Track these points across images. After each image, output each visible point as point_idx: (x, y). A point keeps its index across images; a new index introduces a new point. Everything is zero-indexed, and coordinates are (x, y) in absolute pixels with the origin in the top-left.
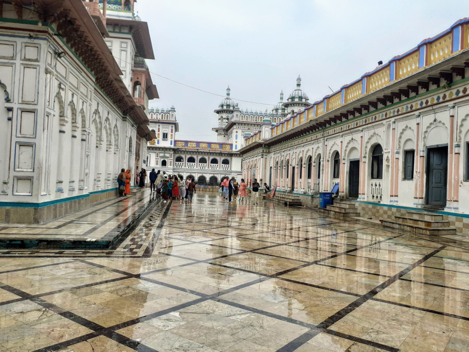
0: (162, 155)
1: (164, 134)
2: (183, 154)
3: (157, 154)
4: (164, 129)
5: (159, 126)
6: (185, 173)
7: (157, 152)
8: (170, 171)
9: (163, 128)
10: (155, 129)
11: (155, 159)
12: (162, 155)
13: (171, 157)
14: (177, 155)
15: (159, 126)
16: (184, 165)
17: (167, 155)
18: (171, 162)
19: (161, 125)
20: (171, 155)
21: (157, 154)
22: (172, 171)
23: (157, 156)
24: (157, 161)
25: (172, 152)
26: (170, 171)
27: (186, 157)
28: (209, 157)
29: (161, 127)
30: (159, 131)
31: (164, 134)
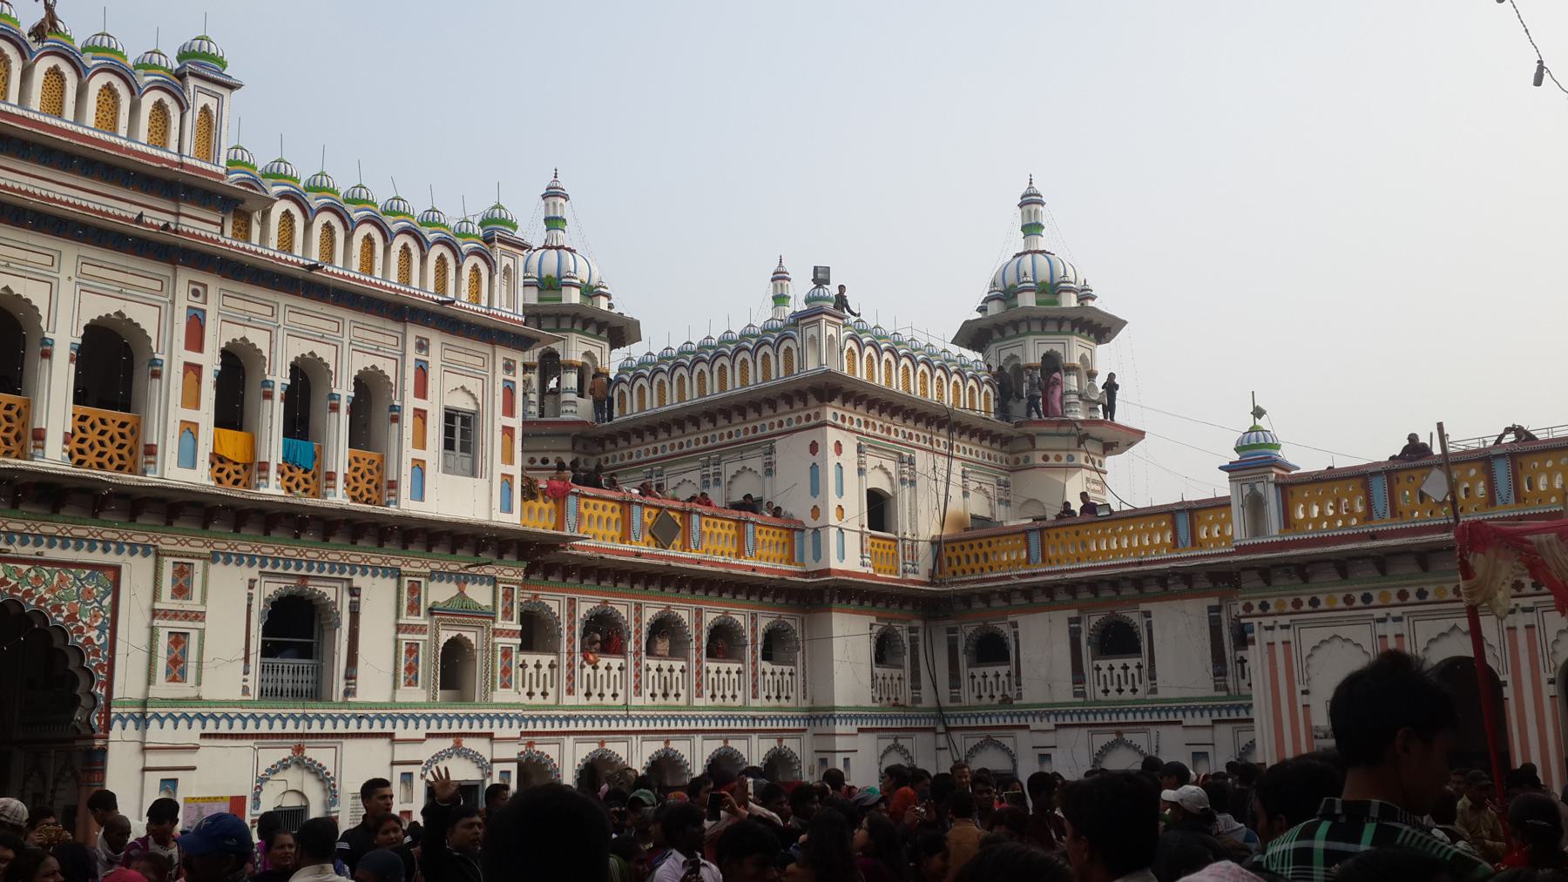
0: (440, 593)
1: (450, 415)
4: (454, 381)
5: (422, 346)
7: (414, 565)
9: (449, 366)
10: (388, 368)
12: (440, 593)
15: (422, 346)
17: (480, 595)
19: (436, 339)
20: (508, 594)
21: (415, 589)
23: (414, 608)
25: (511, 572)
28: (699, 613)
29: (434, 359)
30: (421, 391)
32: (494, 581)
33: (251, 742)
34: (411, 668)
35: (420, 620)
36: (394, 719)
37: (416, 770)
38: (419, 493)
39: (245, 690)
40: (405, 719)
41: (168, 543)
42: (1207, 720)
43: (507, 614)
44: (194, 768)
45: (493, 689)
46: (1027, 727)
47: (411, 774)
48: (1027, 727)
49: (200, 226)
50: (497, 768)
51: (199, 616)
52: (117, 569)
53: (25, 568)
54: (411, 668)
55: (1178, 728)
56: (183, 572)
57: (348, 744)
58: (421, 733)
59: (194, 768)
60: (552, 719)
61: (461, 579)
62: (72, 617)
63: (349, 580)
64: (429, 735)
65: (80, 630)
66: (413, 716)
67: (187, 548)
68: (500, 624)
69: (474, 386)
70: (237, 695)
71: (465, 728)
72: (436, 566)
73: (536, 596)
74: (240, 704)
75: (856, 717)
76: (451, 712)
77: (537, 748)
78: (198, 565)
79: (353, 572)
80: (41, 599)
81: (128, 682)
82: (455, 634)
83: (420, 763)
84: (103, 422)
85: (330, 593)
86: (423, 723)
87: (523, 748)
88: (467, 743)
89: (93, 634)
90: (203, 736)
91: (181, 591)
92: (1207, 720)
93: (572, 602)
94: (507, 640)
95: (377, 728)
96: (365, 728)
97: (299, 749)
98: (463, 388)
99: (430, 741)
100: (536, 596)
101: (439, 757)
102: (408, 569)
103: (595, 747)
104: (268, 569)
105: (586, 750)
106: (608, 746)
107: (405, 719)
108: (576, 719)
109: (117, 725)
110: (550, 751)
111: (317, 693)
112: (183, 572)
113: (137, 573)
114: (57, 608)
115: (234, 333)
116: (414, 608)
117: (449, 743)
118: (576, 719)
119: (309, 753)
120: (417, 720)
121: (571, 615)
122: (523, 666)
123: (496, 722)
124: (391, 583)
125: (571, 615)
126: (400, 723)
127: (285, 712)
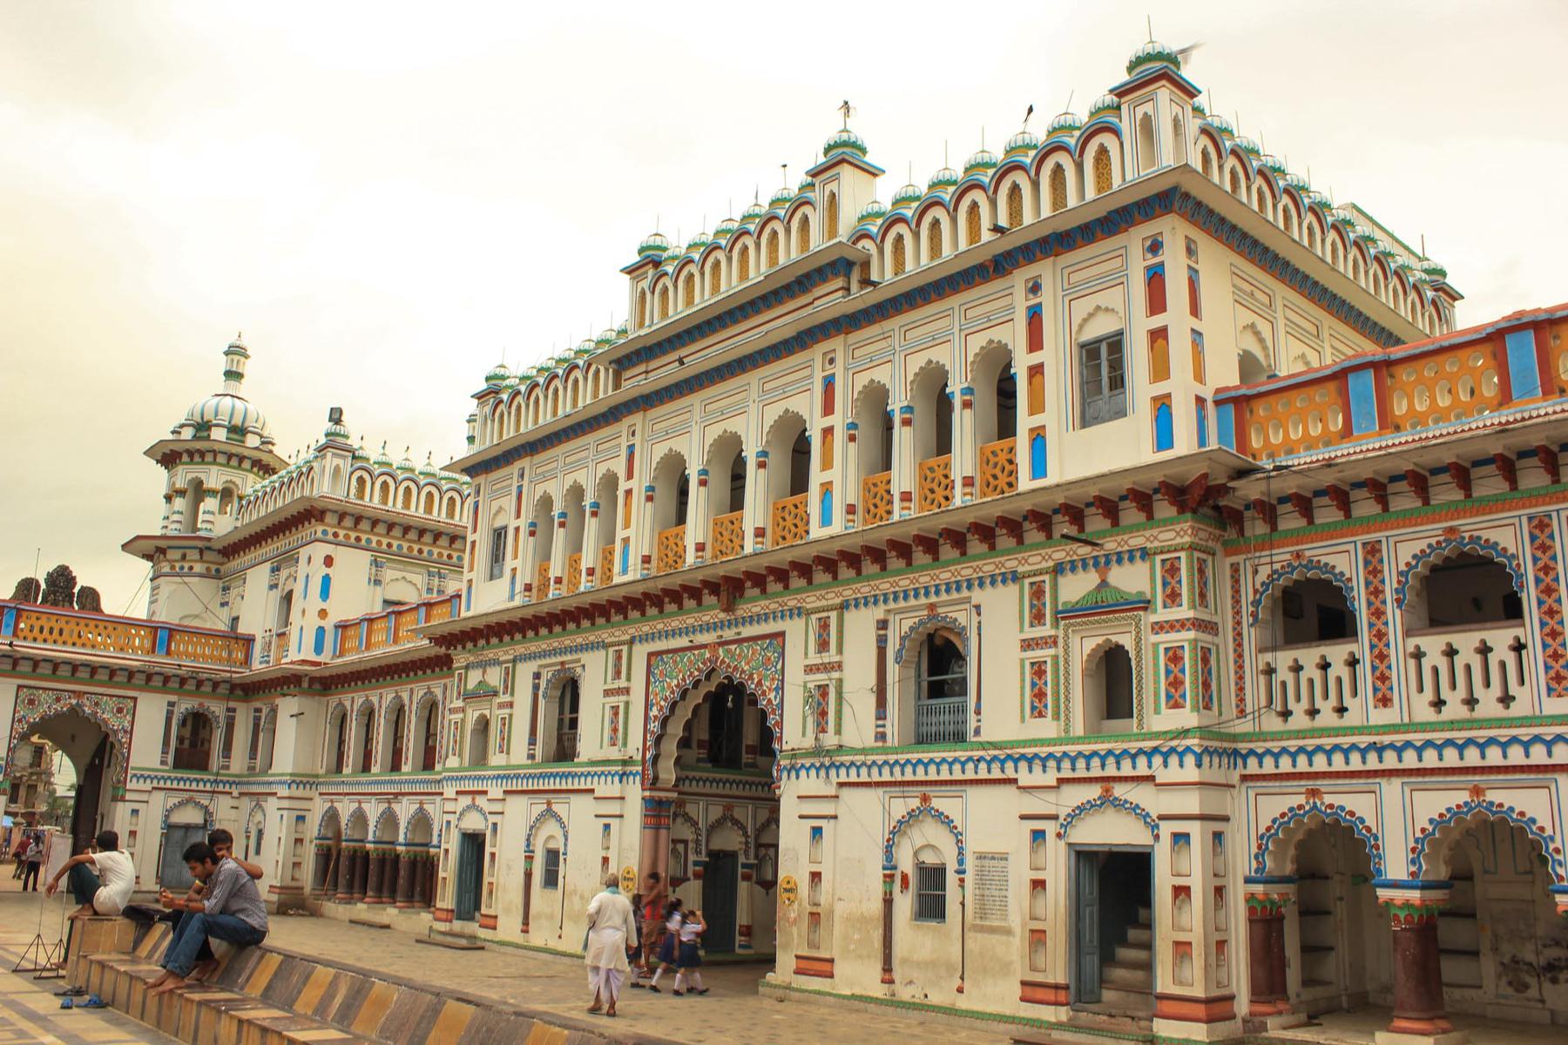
1: (1090, 351)
2: (1330, 532)
3: (1038, 592)
6: (1392, 789)
7: (1036, 560)
8: (1173, 773)
10: (1001, 334)
11: (1016, 653)
12: (1076, 587)
13: (1173, 597)
14: (1267, 566)
16: (1365, 670)
17: (1132, 579)
18: (1175, 656)
19: (1045, 270)
20: (1172, 570)
21: (1038, 592)
22: (1190, 773)
23: (1038, 618)
24: (1039, 670)
25: (1175, 533)
26: (1173, 773)
27: (1377, 561)
31: (1090, 351)
32: (1145, 554)
33: (880, 791)
34: (1176, 683)
35: (1046, 630)
36: (1016, 761)
37: (1050, 828)
38: (1039, 468)
39: (881, 737)
40: (1030, 761)
41: (811, 601)
42: (148, 786)
43: (1173, 597)
44: (801, 817)
45: (1157, 711)
46: (1150, 779)
47: (1186, 836)
48: (1015, 781)
49: (829, 301)
50: (1167, 829)
51: (839, 666)
52: (782, 634)
53: (733, 647)
54: (1176, 683)
55: (1010, 790)
56: (824, 625)
57: (973, 793)
58: (1050, 778)
59: (801, 817)
60: (1380, 750)
61: (1102, 564)
62: (759, 683)
63: (968, 600)
64: (1061, 781)
65: (764, 693)
66: (1023, 757)
67: (824, 603)
68: (1162, 614)
69: (1113, 298)
70: (870, 742)
71: (1111, 770)
72: (1059, 555)
73: (1298, 555)
74: (872, 751)
75: (507, 777)
76: (914, 757)
77: (1328, 799)
78: (833, 615)
79: (969, 587)
80: (743, 671)
81: (794, 732)
82: (1100, 640)
83: (1055, 817)
84: (796, 506)
85: (962, 618)
86: (1052, 764)
87: (1301, 800)
88: (1119, 791)
89: (772, 696)
90: (841, 785)
91: (823, 646)
92: (148, 786)
93: (1372, 550)
94: (1173, 636)
95: (996, 774)
96: (983, 774)
97: (925, 799)
98: (1098, 308)
99: (1067, 790)
100: (1298, 555)
101: (1081, 810)
102: (1027, 568)
103: (1463, 797)
104: (892, 605)
105: (1435, 803)
106: (1493, 796)
107: (1030, 761)
108: (1380, 750)
109: (785, 774)
110: (1358, 804)
111: (959, 737)
112: (824, 625)
113: (797, 633)
114: (751, 677)
115: (862, 380)
116: (1038, 618)
117: (1094, 792)
118: (1399, 750)
119: (936, 803)
120: (1044, 761)
121: (1374, 571)
122: (1270, 671)
123: (1157, 760)
124: (1012, 589)
125: (1374, 571)
126: (1023, 765)
127: (937, 756)
